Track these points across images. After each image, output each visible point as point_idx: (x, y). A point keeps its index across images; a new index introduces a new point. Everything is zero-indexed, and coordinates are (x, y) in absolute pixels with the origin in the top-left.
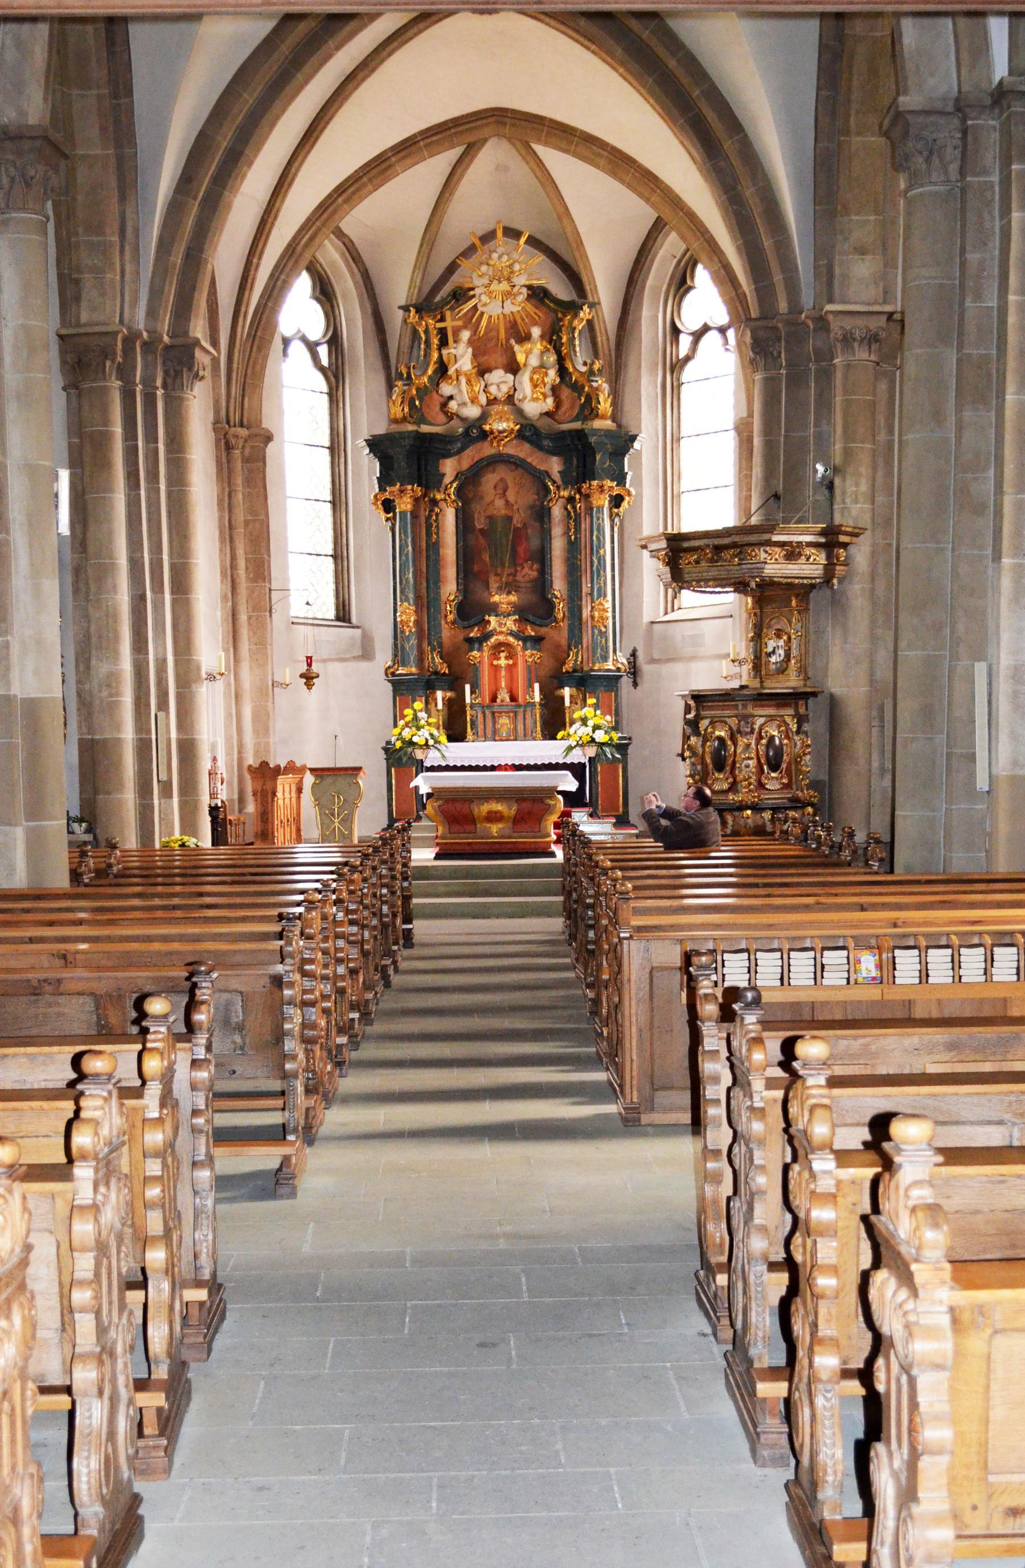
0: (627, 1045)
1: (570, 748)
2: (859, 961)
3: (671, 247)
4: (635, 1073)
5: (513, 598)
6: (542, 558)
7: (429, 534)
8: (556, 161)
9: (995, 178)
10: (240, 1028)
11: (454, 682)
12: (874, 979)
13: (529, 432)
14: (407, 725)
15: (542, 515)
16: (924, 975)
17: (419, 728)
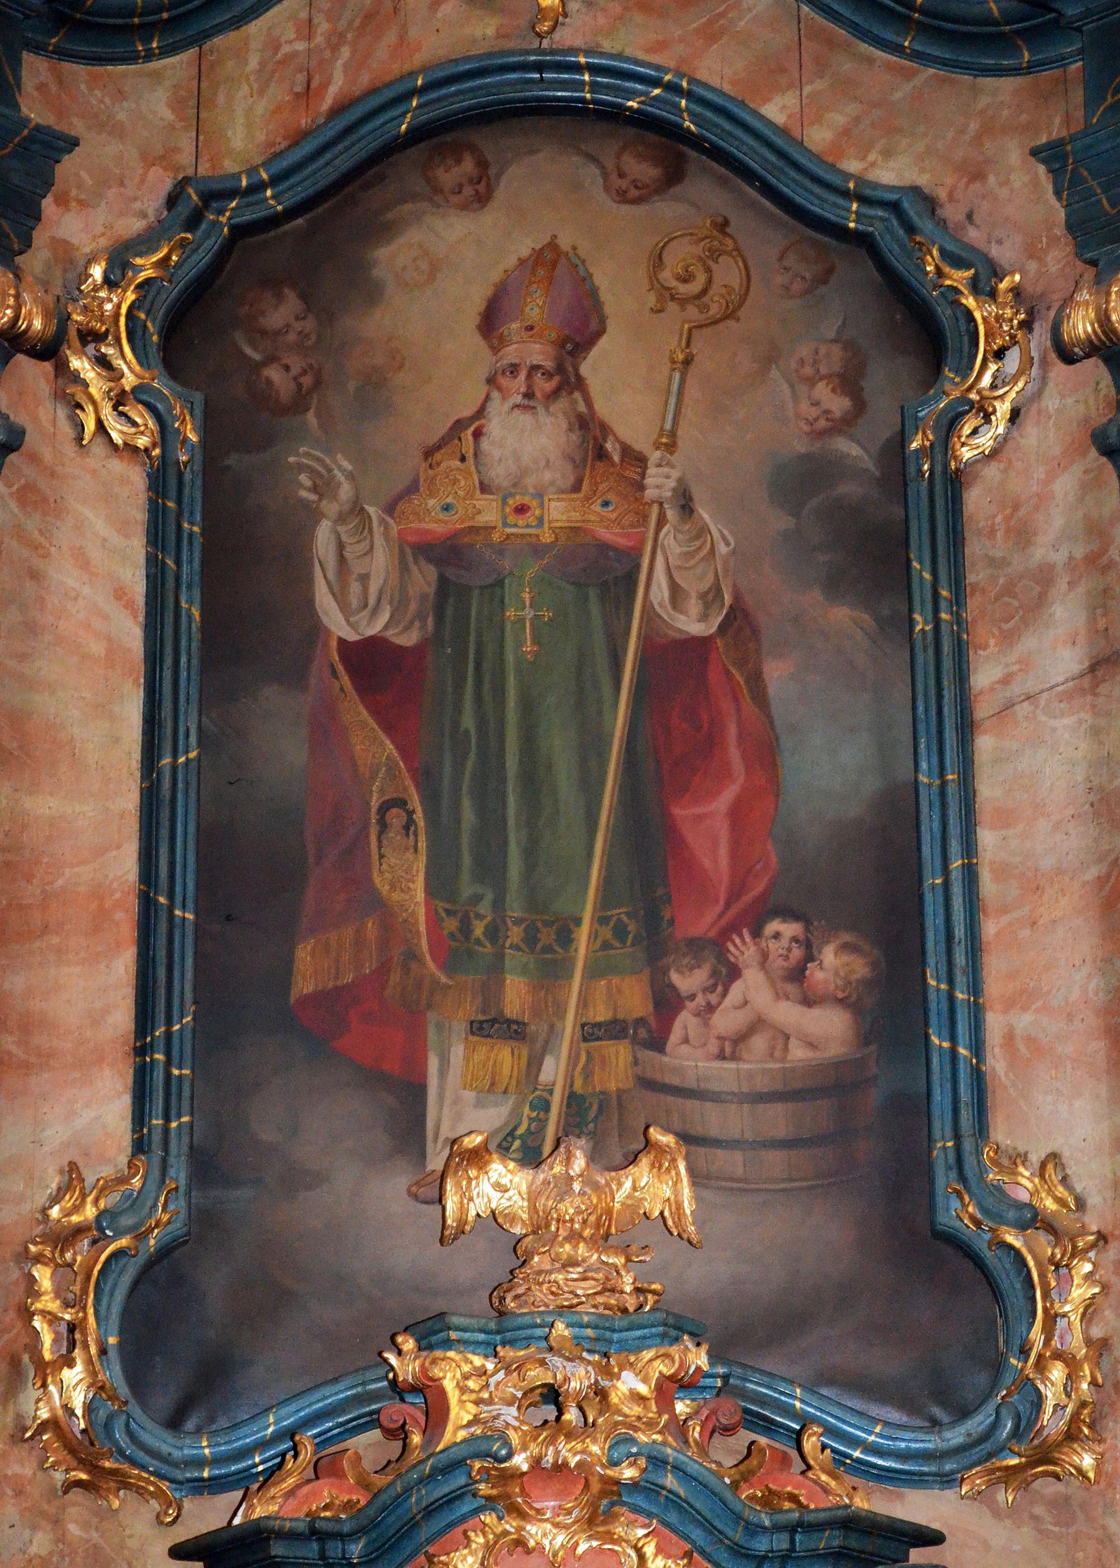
5: (656, 1187)
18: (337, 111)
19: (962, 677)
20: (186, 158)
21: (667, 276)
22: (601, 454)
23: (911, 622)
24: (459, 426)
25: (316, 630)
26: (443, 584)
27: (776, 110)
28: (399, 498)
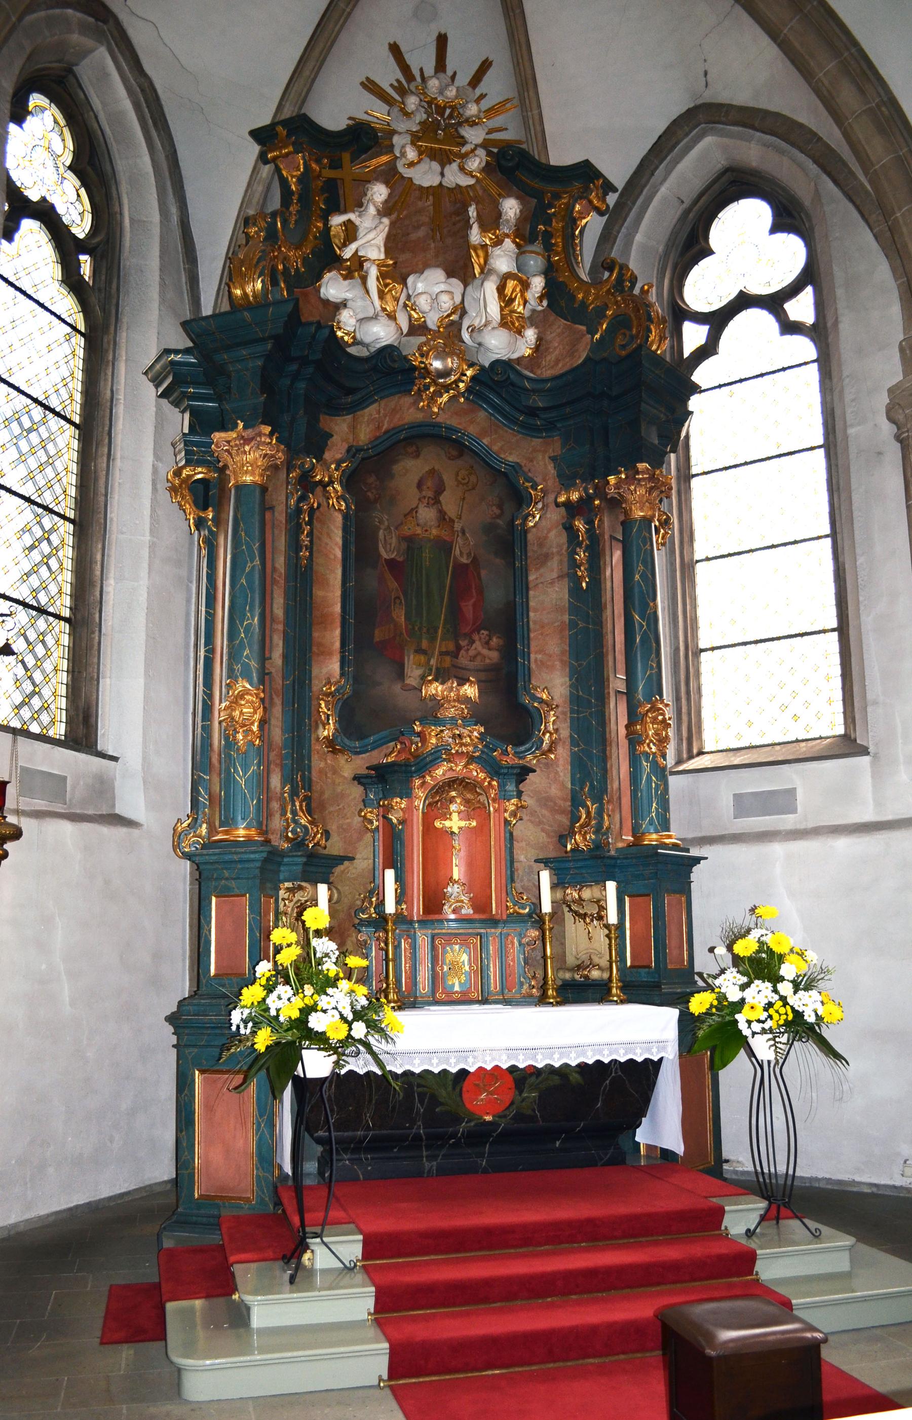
5: (470, 691)
6: (510, 627)
7: (295, 545)
14: (281, 975)
15: (510, 544)
18: (386, 432)
19: (527, 578)
20: (351, 440)
21: (459, 478)
22: (444, 519)
23: (515, 564)
24: (412, 509)
25: (380, 556)
26: (408, 548)
27: (486, 441)
28: (399, 525)
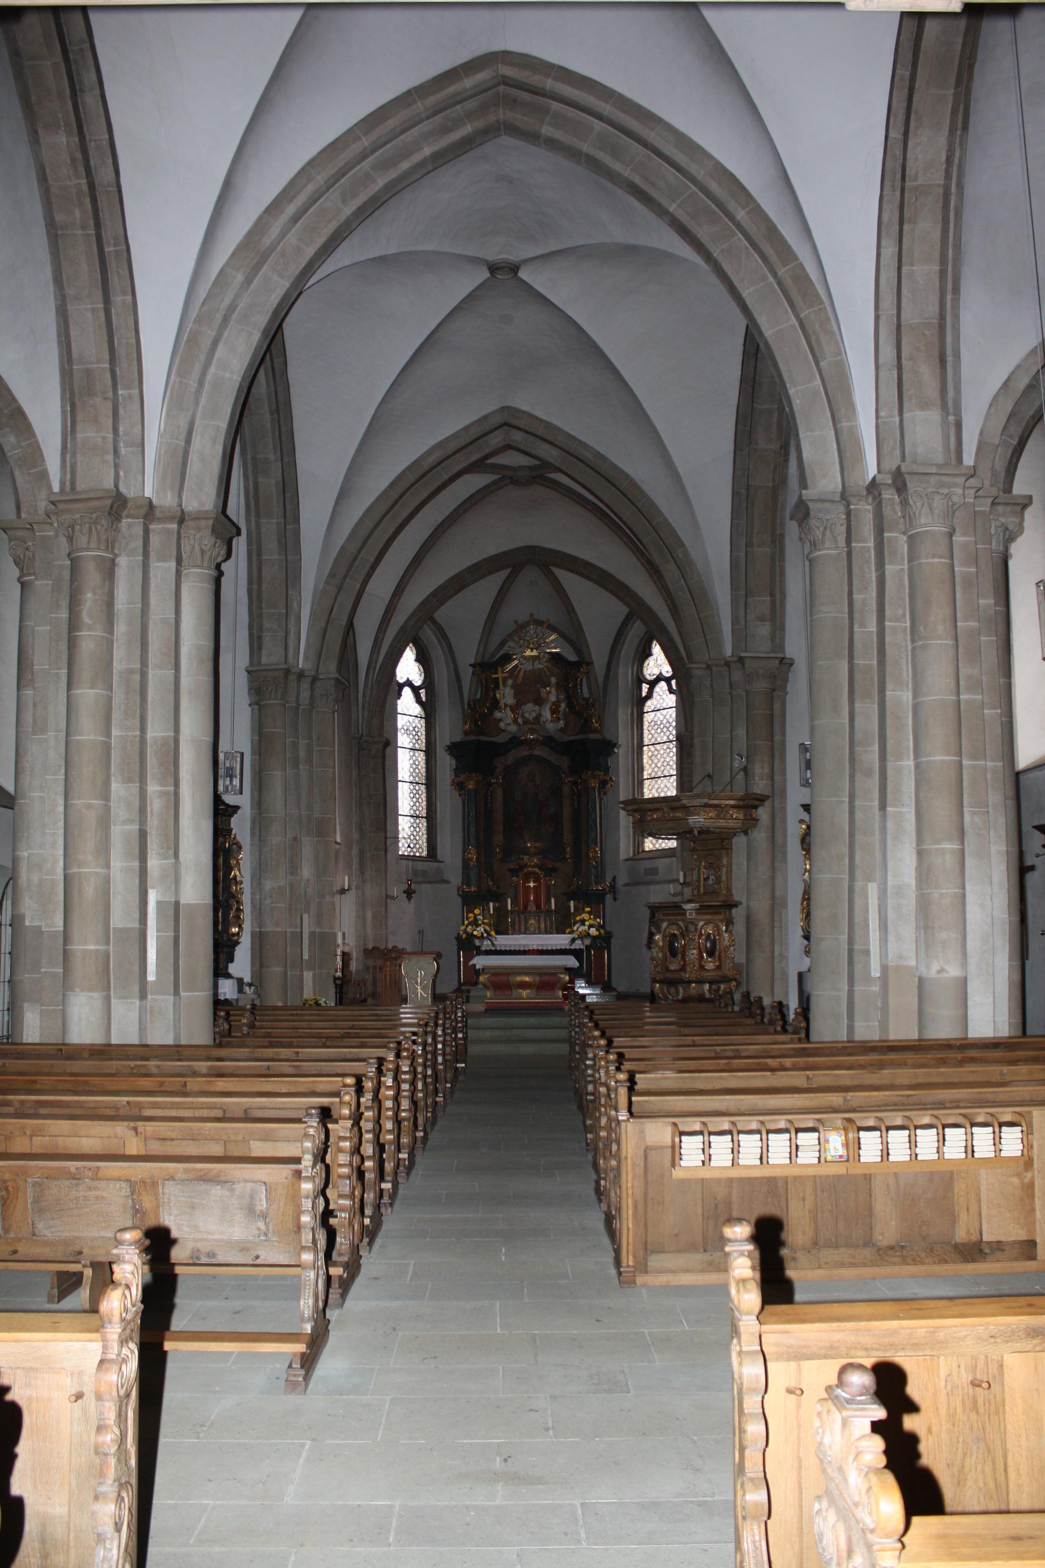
0: (624, 1215)
1: (573, 940)
2: (827, 1141)
3: (637, 629)
4: (631, 1240)
8: (566, 578)
9: (871, 544)
10: (264, 1216)
11: (498, 897)
12: (841, 1157)
13: (549, 741)
16: (886, 1153)
17: (478, 926)
